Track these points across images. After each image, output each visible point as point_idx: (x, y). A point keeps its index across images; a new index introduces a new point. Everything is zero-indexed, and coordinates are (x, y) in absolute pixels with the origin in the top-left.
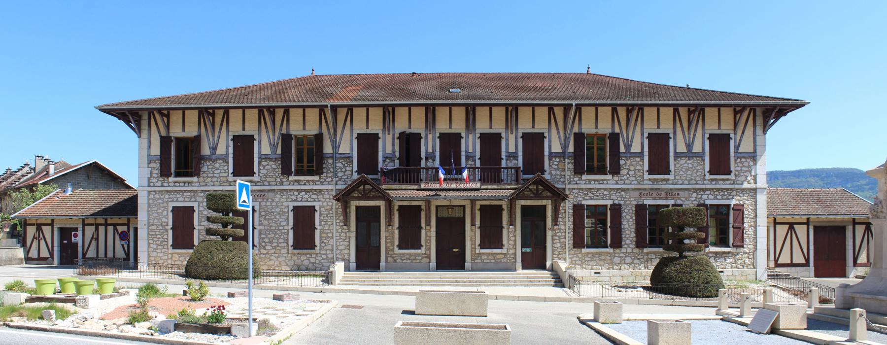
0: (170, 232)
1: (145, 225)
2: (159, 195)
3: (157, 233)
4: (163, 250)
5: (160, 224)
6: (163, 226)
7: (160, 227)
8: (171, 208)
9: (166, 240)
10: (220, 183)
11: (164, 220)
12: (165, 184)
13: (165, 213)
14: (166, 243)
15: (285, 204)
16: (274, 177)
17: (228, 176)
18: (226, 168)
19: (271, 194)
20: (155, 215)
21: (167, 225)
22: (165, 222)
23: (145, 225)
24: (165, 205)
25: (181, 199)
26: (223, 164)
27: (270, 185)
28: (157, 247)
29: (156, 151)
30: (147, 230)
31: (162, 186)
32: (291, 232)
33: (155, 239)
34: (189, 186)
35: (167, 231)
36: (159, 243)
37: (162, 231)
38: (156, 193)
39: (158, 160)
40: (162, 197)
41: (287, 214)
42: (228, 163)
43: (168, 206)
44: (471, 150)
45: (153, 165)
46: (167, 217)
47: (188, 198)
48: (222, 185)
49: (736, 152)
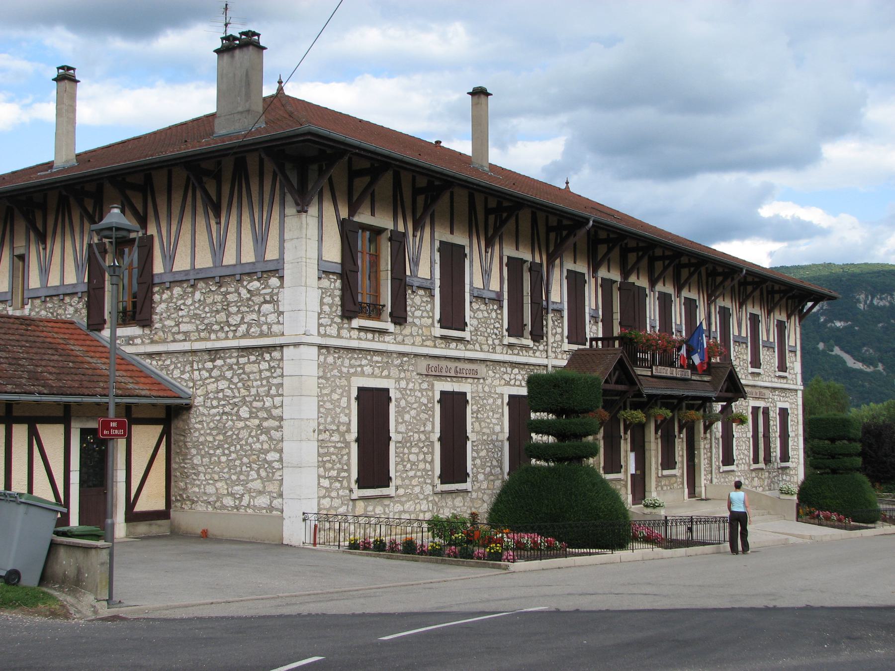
0: (354, 447)
1: (314, 431)
2: (334, 357)
3: (332, 449)
4: (341, 492)
5: (335, 428)
6: (342, 435)
7: (336, 437)
8: (354, 393)
9: (345, 467)
10: (423, 341)
11: (343, 419)
12: (344, 333)
13: (345, 399)
14: (346, 474)
15: (499, 390)
16: (486, 335)
17: (433, 325)
18: (429, 307)
19: (482, 369)
20: (329, 405)
21: (348, 431)
22: (344, 424)
23: (314, 431)
24: (344, 382)
25: (368, 370)
26: (425, 299)
27: (482, 350)
28: (331, 484)
29: (333, 253)
30: (316, 444)
31: (339, 336)
32: (507, 445)
33: (329, 465)
34: (379, 341)
35: (347, 445)
36: (334, 473)
37: (339, 445)
38: (329, 353)
39: (334, 273)
40: (339, 362)
41: (500, 411)
42: (432, 296)
43: (349, 386)
44: (652, 318)
45: (325, 283)
46: (347, 411)
47: (379, 367)
48: (425, 343)
49: (788, 345)
